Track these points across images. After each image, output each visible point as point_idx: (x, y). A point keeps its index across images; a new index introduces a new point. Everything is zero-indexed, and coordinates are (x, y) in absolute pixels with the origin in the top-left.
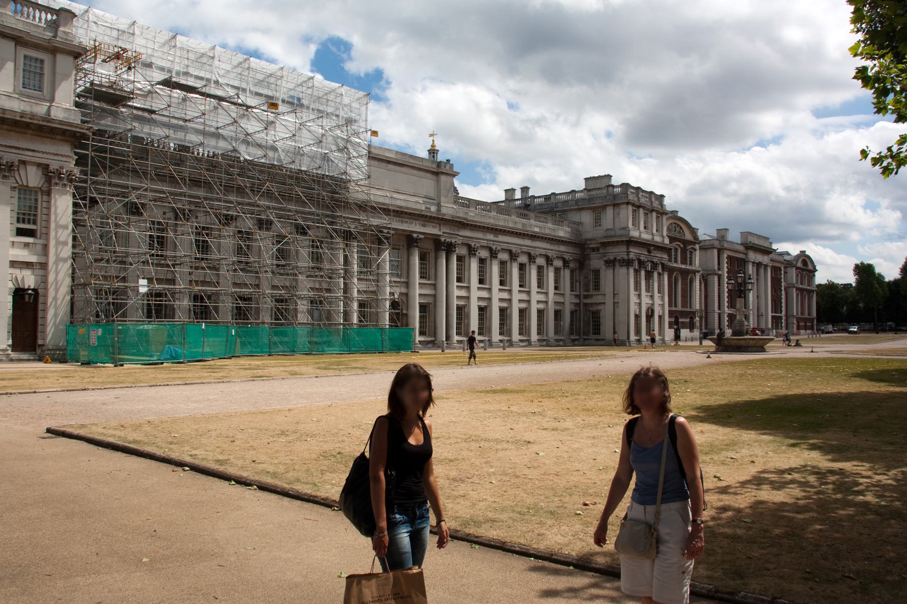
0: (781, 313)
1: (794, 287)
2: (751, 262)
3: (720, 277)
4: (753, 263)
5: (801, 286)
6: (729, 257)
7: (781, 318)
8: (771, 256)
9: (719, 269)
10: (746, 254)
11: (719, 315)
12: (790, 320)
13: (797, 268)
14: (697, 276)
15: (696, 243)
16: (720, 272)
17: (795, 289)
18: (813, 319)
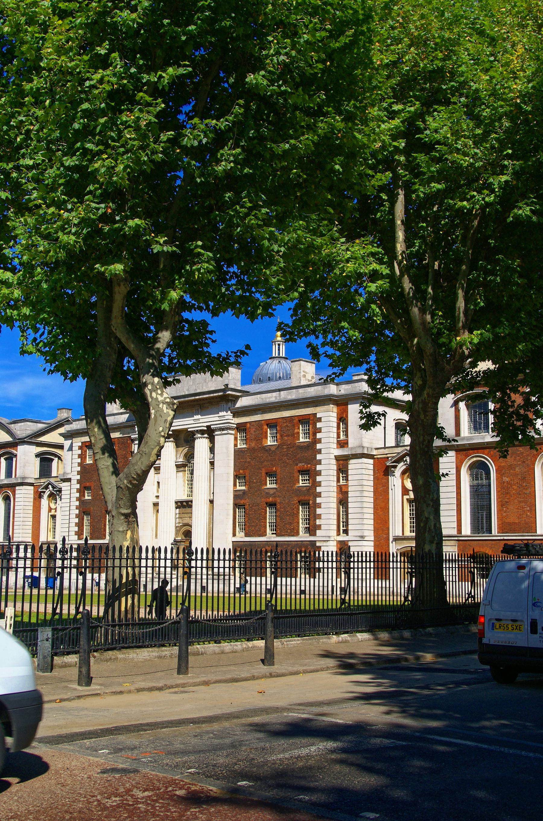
14: (17, 492)
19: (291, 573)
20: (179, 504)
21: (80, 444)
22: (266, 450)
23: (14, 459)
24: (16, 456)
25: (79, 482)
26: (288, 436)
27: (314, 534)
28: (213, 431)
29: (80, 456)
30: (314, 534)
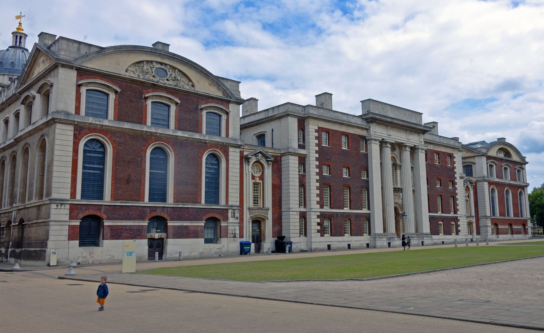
0: (455, 212)
1: (485, 181)
2: (376, 140)
3: (302, 160)
4: (383, 143)
5: (497, 180)
6: (320, 130)
7: (456, 220)
8: (427, 136)
9: (302, 147)
10: (367, 130)
11: (303, 216)
12: (482, 222)
13: (489, 158)
14: (230, 154)
15: (229, 102)
16: (302, 152)
17: (486, 184)
18: (526, 221)
19: (450, 234)
20: (397, 189)
21: (317, 128)
22: (436, 167)
23: (224, 117)
24: (227, 113)
25: (317, 159)
26: (444, 161)
27: (457, 214)
28: (418, 149)
29: (316, 138)
30: (457, 214)
